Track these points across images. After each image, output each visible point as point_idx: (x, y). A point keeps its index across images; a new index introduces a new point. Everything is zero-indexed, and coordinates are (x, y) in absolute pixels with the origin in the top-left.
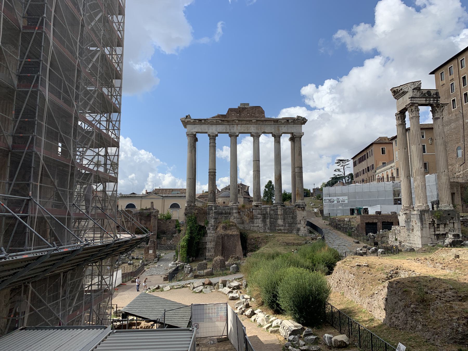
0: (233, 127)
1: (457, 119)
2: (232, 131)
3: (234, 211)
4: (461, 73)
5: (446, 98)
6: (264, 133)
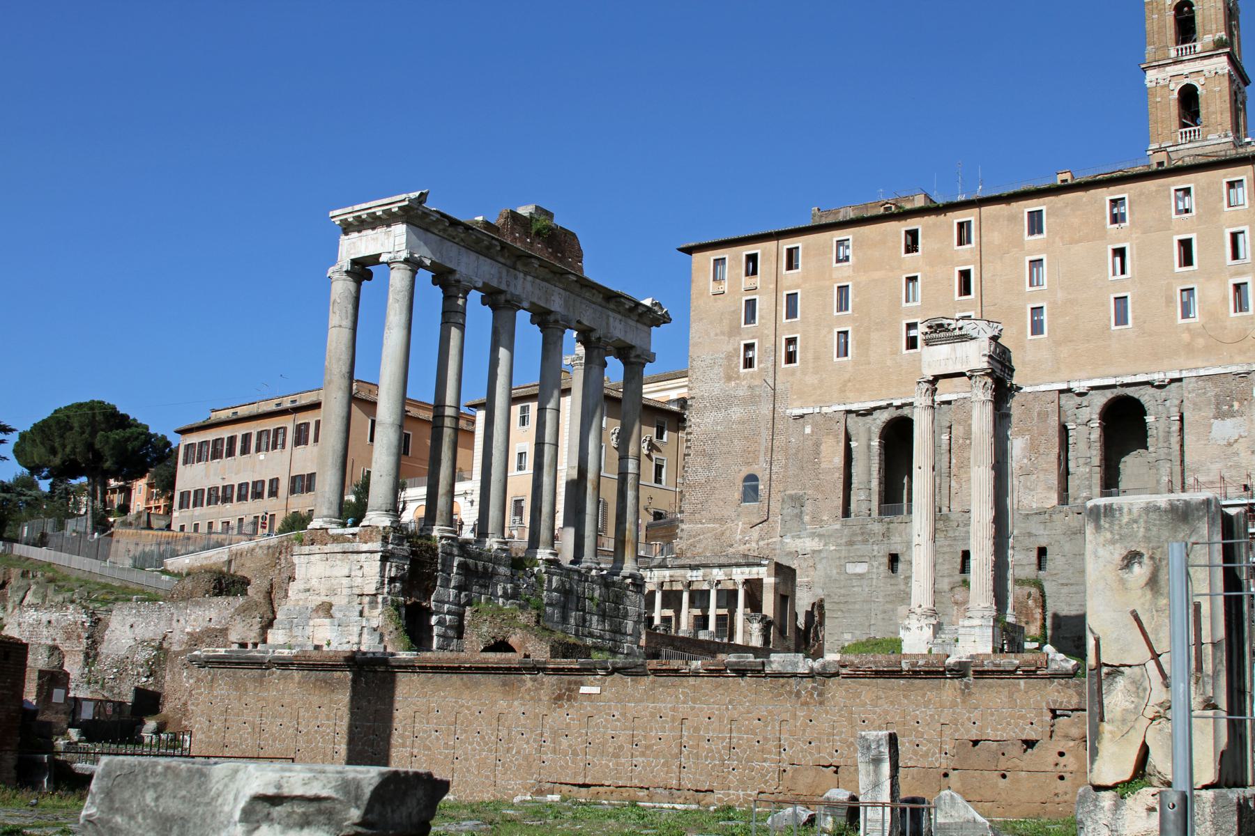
0: (516, 278)
1: (753, 399)
2: (512, 289)
4: (781, 283)
5: (723, 333)
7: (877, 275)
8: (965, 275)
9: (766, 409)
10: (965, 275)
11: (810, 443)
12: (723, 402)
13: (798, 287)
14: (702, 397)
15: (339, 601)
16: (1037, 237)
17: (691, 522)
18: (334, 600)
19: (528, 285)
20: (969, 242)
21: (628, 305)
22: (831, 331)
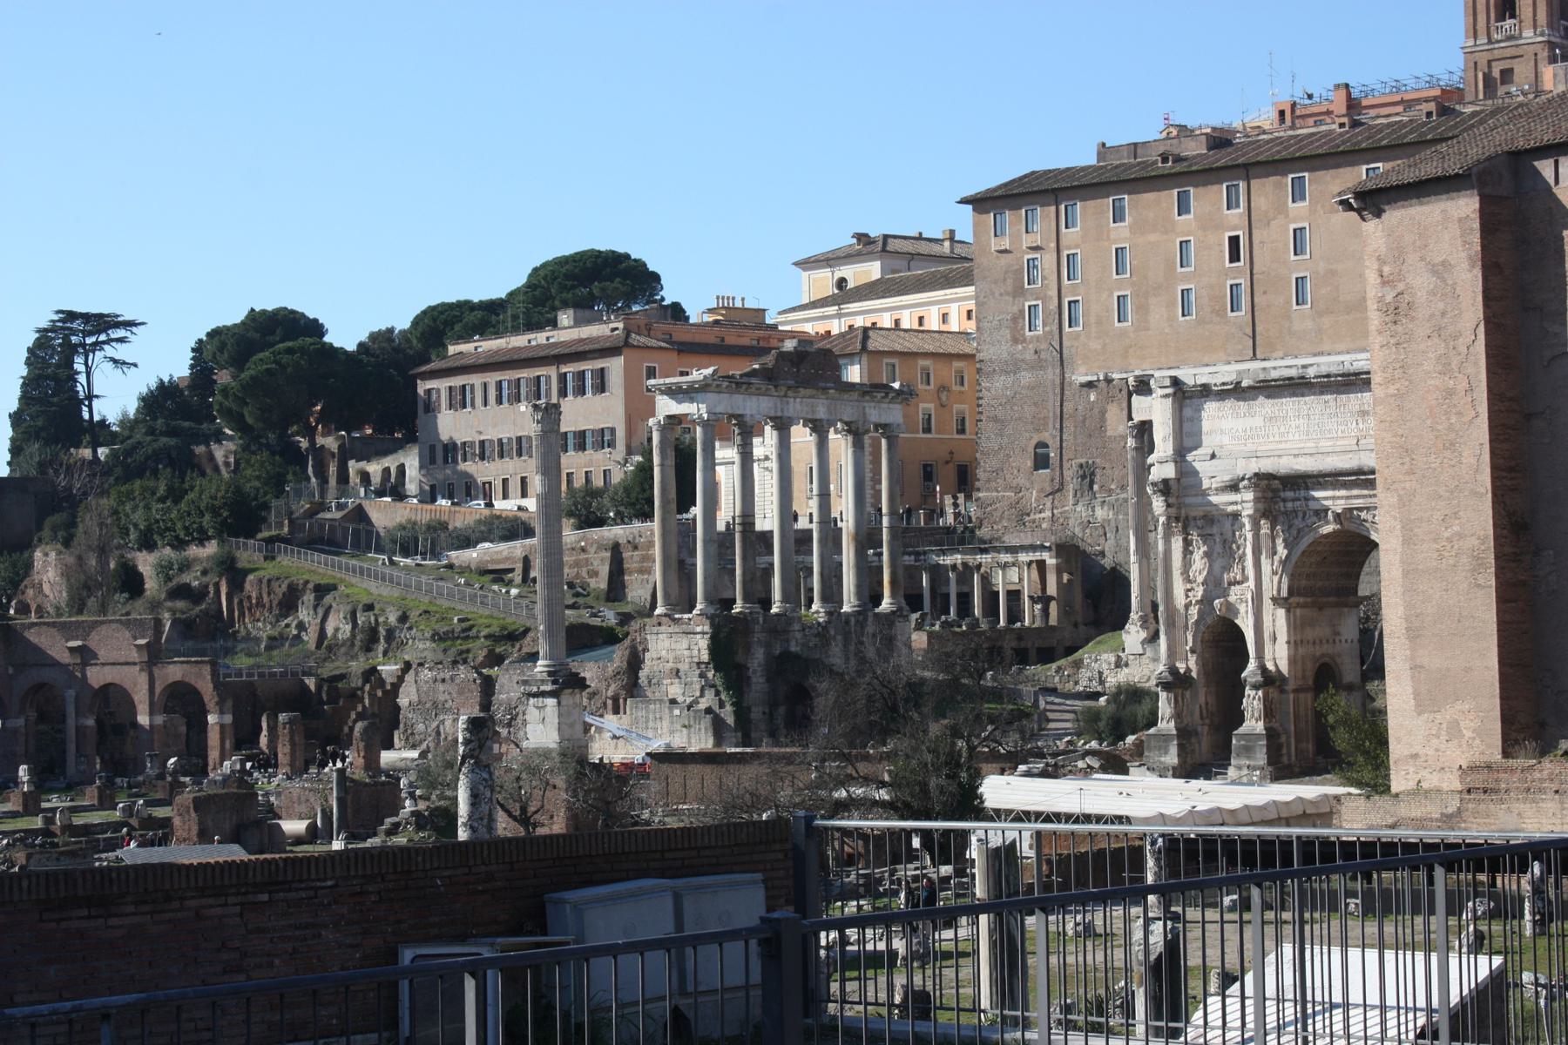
2: (786, 414)
4: (1063, 242)
5: (1008, 294)
7: (1152, 237)
8: (1234, 241)
9: (1052, 375)
10: (1234, 241)
11: (1096, 411)
12: (1013, 367)
13: (1077, 247)
14: (991, 361)
15: (683, 667)
16: (1300, 204)
17: (988, 490)
18: (680, 666)
19: (798, 407)
20: (1238, 206)
22: (1111, 295)
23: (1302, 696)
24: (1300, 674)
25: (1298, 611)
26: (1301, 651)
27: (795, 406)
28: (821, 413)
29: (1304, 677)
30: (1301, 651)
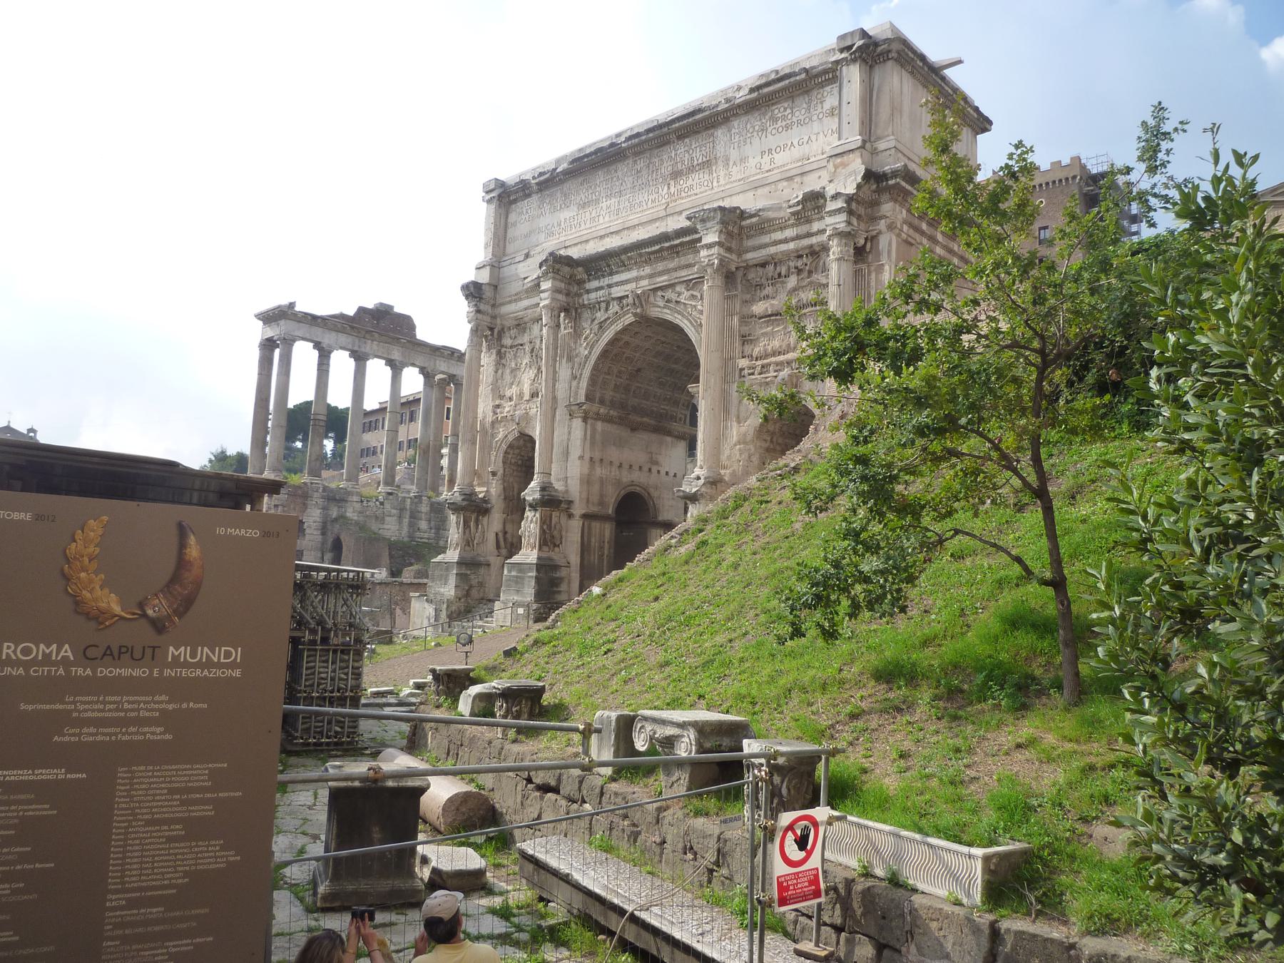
3: (355, 498)
6: (413, 365)
19: (375, 347)
21: (446, 353)
23: (596, 525)
24: (595, 499)
25: (599, 425)
26: (599, 471)
27: (368, 347)
28: (396, 355)
29: (601, 503)
30: (599, 471)
